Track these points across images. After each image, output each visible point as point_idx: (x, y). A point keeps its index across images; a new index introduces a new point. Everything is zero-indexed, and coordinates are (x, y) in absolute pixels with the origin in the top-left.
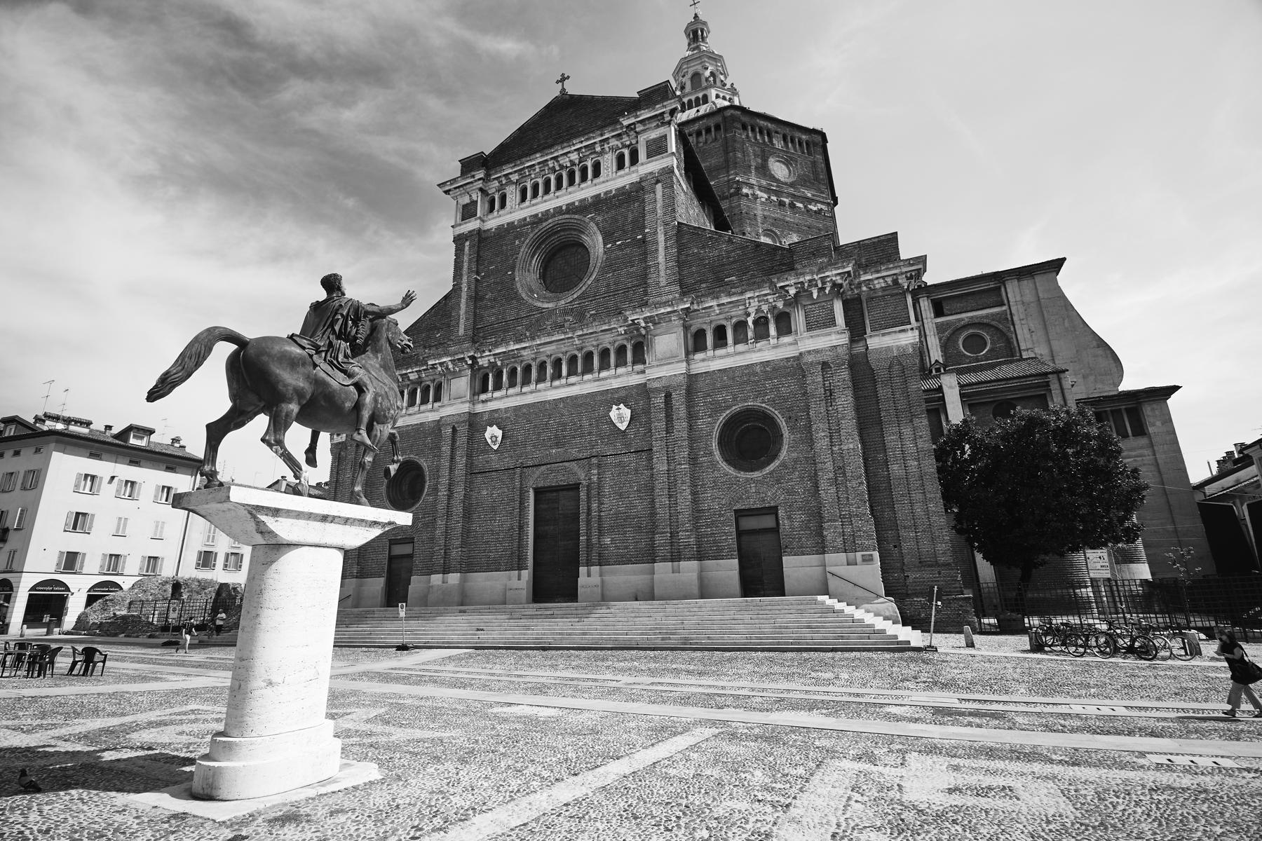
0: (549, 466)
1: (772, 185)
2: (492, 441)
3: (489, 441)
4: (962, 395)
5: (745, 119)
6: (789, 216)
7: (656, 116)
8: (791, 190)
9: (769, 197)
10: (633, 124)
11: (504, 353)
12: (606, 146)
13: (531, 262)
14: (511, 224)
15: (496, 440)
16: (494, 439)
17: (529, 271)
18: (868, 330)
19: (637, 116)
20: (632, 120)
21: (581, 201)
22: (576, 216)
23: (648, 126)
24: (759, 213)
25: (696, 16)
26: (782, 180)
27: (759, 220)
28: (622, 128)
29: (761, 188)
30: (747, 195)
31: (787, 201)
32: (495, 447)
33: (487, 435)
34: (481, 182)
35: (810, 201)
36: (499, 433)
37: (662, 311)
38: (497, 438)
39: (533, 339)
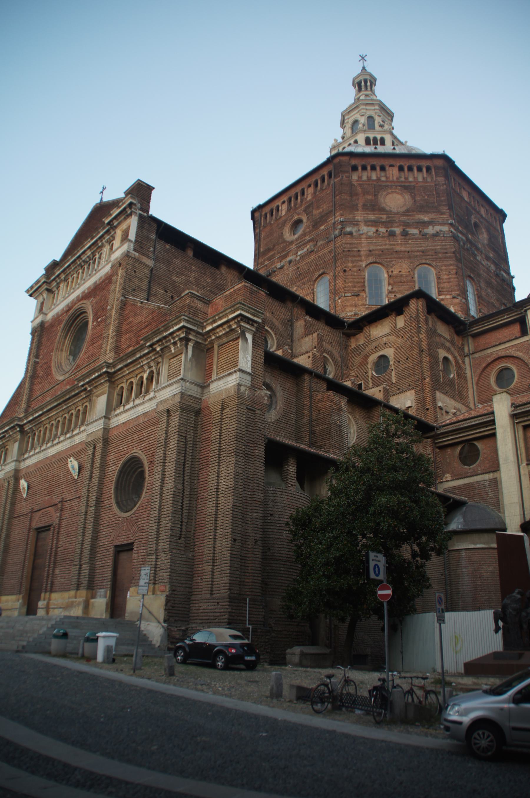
0: (43, 511)
1: (381, 218)
4: (514, 416)
5: (354, 162)
6: (399, 245)
8: (403, 218)
9: (377, 231)
13: (64, 342)
14: (57, 314)
17: (62, 350)
18: (214, 377)
19: (111, 215)
20: (110, 219)
23: (120, 220)
24: (364, 249)
25: (364, 68)
26: (395, 210)
27: (363, 255)
29: (368, 223)
30: (351, 233)
31: (398, 230)
34: (45, 284)
35: (431, 223)
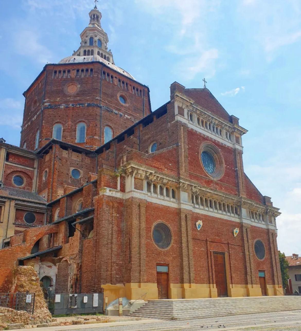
2: (198, 227)
3: (197, 226)
7: (241, 131)
10: (236, 128)
11: (203, 190)
12: (225, 127)
15: (200, 227)
16: (199, 226)
21: (218, 142)
22: (217, 147)
25: (96, 7)
28: (232, 126)
32: (199, 229)
33: (197, 223)
36: (201, 224)
37: (249, 202)
38: (200, 225)
39: (215, 191)
